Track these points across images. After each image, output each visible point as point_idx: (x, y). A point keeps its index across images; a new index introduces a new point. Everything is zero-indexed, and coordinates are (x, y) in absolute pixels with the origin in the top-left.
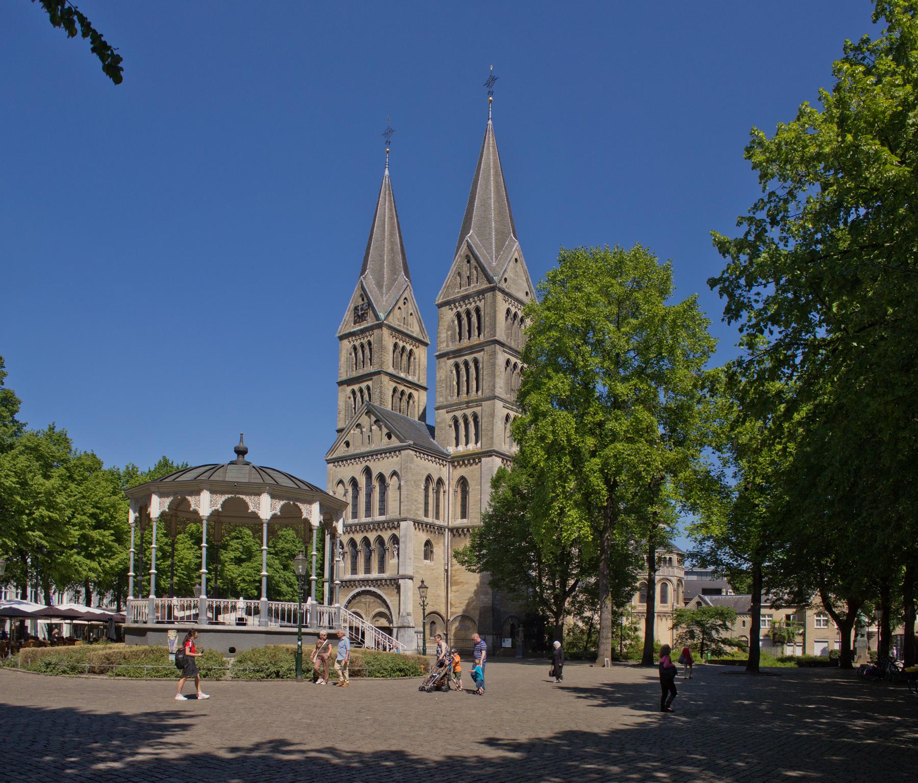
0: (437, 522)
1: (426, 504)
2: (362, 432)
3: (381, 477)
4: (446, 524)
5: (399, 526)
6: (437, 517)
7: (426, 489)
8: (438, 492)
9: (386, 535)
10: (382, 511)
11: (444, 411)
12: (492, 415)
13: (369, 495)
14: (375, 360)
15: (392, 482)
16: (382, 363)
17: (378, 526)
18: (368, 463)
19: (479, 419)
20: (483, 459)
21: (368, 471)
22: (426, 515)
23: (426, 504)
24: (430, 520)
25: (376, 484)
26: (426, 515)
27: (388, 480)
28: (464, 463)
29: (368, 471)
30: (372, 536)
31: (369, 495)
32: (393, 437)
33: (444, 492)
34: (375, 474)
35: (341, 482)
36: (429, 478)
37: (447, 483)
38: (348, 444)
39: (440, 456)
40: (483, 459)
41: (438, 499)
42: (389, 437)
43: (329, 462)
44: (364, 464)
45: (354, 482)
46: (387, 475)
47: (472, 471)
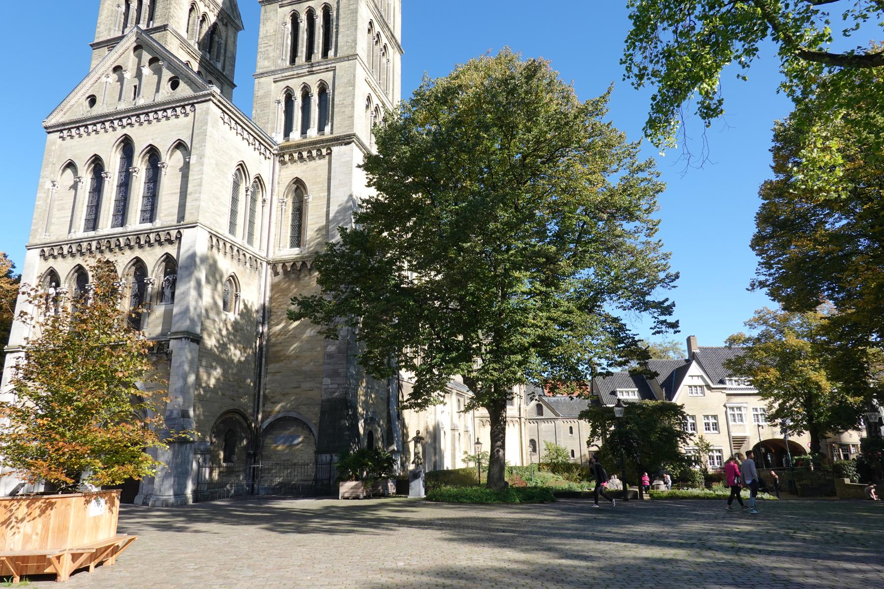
0: (247, 245)
1: (234, 213)
2: (121, 80)
3: (153, 154)
4: (264, 254)
5: (179, 238)
6: (250, 241)
7: (236, 185)
8: (254, 200)
9: (152, 258)
10: (150, 213)
11: (270, 79)
12: (352, 84)
13: (125, 185)
14: (158, 11)
15: (171, 162)
16: (167, 16)
17: (139, 240)
18: (128, 131)
19: (330, 91)
20: (335, 149)
21: (127, 145)
22: (232, 230)
23: (234, 213)
24: (239, 238)
25: (140, 166)
26: (232, 230)
27: (165, 157)
28: (301, 158)
29: (127, 145)
30: (122, 261)
31: (125, 185)
32: (182, 84)
33: (264, 201)
34: (139, 147)
35: (71, 165)
36: (242, 168)
37: (268, 187)
38: (92, 100)
39: (261, 141)
40: (335, 149)
41: (253, 211)
42: (175, 85)
43: (49, 130)
44: (120, 132)
45: (97, 164)
46: (163, 148)
47: (315, 169)
